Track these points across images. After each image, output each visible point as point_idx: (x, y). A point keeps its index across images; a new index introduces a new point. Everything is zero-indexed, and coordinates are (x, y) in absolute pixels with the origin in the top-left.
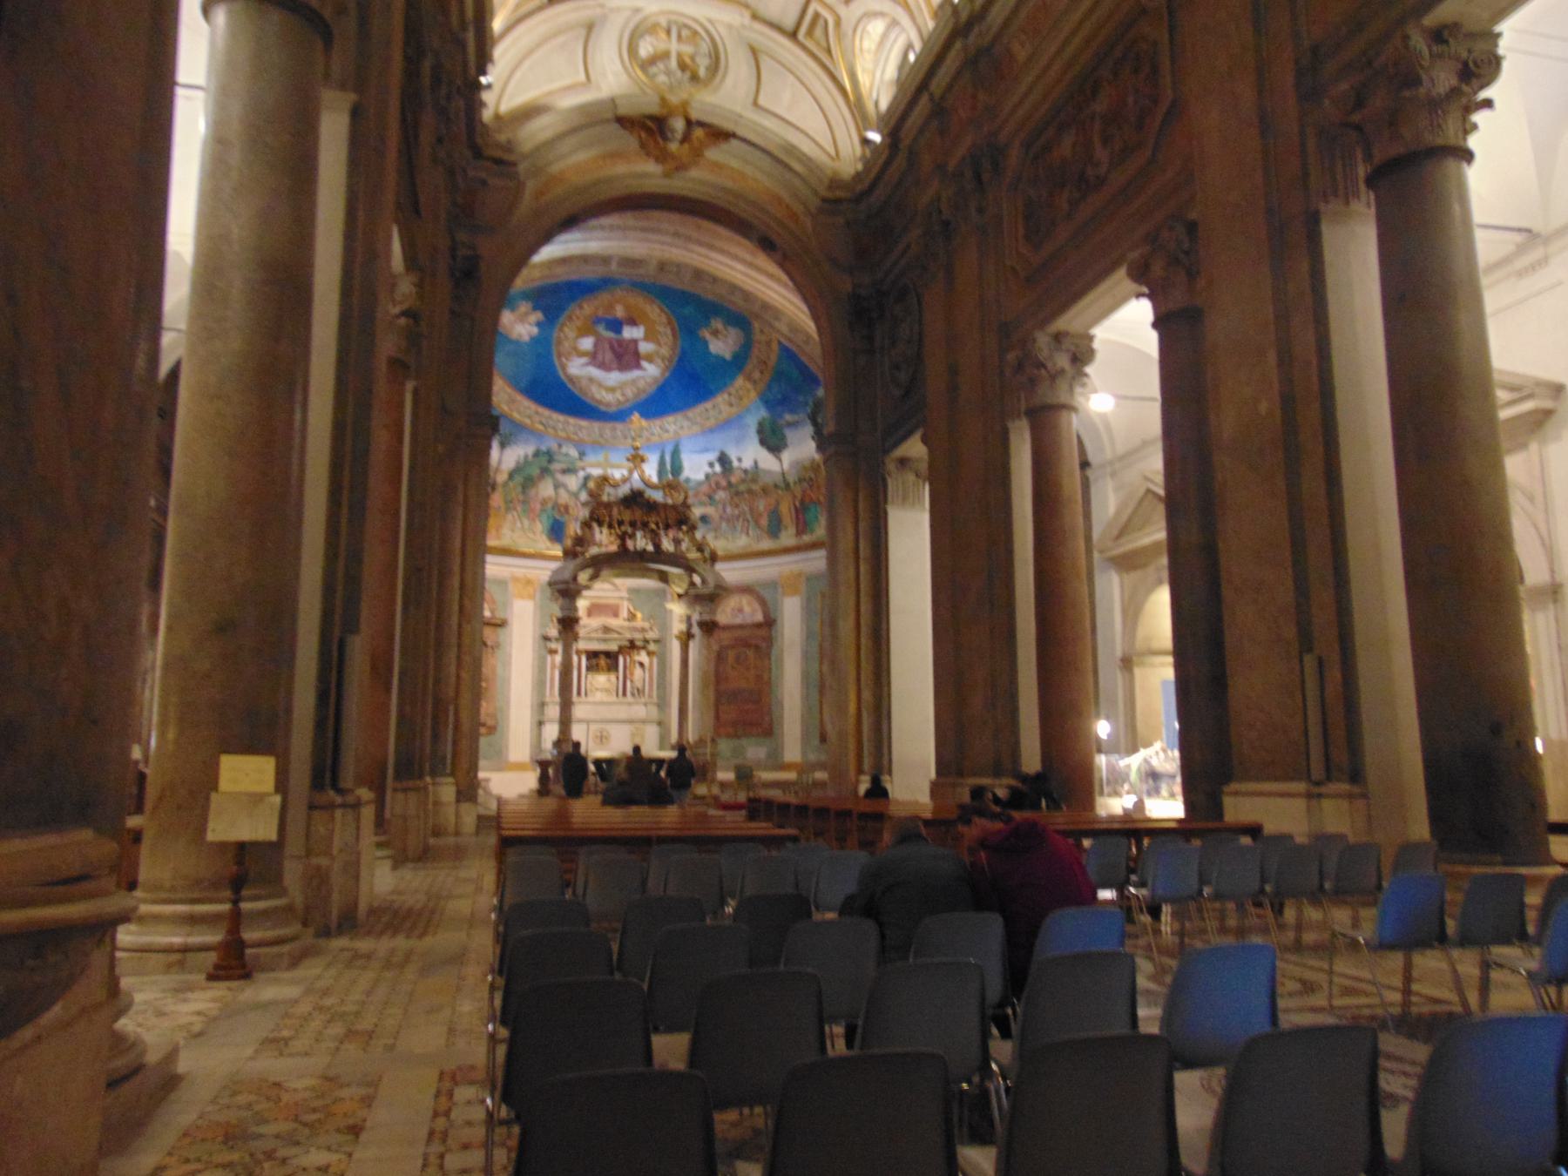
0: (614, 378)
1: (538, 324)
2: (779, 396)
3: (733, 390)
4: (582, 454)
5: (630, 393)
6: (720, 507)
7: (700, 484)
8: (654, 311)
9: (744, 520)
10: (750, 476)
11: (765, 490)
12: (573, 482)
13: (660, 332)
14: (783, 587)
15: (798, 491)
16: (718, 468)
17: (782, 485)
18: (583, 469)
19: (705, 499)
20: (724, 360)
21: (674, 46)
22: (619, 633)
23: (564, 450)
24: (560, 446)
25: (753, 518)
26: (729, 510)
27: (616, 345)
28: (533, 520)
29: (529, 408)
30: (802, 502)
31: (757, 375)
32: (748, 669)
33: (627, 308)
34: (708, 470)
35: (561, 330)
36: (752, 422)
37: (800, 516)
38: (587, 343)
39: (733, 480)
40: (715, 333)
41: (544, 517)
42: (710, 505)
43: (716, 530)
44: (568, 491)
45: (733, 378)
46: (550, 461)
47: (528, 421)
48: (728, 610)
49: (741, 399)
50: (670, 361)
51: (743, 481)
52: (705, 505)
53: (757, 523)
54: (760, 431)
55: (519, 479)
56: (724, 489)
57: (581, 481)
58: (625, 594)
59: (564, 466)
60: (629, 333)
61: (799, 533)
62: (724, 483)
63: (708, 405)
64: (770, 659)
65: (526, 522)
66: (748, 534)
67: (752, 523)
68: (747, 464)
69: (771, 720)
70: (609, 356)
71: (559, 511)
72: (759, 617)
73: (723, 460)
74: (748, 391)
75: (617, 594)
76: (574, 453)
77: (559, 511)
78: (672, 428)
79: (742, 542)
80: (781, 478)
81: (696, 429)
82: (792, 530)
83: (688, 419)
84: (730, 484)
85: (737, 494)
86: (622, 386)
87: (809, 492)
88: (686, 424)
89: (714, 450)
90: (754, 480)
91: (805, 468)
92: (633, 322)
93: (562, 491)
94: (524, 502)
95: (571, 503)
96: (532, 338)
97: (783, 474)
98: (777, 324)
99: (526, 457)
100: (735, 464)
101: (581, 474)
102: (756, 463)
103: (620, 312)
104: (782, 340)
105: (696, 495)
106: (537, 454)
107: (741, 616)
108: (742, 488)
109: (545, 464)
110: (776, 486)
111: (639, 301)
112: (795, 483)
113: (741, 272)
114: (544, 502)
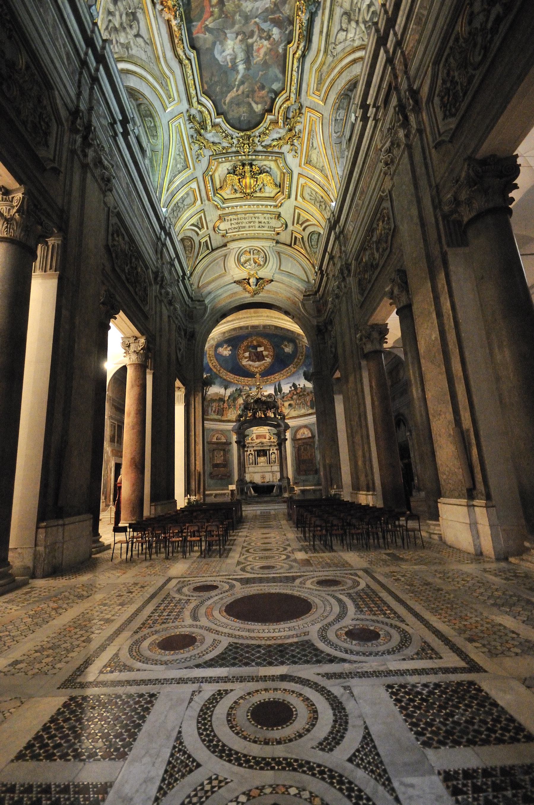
0: (257, 364)
1: (231, 350)
4: (250, 389)
5: (263, 368)
7: (288, 394)
8: (265, 342)
21: (252, 256)
31: (300, 357)
33: (257, 342)
36: (301, 372)
38: (247, 354)
40: (286, 346)
43: (294, 408)
45: (294, 359)
46: (241, 392)
55: (232, 398)
60: (259, 349)
68: (302, 386)
70: (254, 358)
72: (310, 435)
73: (294, 385)
76: (248, 389)
78: (277, 377)
79: (303, 411)
86: (260, 366)
90: (305, 391)
92: (260, 346)
94: (234, 405)
103: (255, 343)
106: (236, 390)
111: (261, 339)
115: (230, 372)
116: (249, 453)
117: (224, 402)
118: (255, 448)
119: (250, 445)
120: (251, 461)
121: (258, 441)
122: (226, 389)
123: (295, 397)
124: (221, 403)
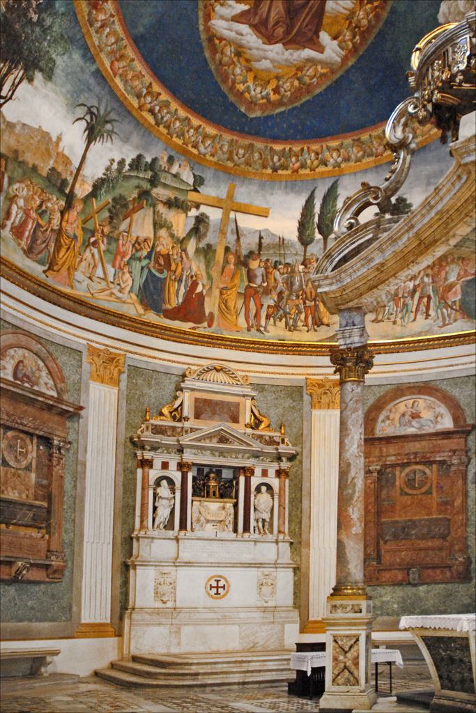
4: (199, 181)
9: (421, 298)
12: (181, 223)
18: (197, 207)
23: (175, 169)
24: (171, 160)
29: (139, 76)
44: (172, 236)
46: (154, 182)
47: (135, 103)
53: (443, 298)
55: (106, 198)
57: (191, 223)
66: (428, 316)
76: (188, 177)
77: (157, 261)
93: (163, 232)
94: (112, 239)
95: (175, 254)
99: (122, 163)
101: (193, 213)
106: (137, 163)
109: (146, 186)
114: (137, 244)
115: (137, 41)
117: (70, 199)
122: (92, 134)
124: (56, 203)
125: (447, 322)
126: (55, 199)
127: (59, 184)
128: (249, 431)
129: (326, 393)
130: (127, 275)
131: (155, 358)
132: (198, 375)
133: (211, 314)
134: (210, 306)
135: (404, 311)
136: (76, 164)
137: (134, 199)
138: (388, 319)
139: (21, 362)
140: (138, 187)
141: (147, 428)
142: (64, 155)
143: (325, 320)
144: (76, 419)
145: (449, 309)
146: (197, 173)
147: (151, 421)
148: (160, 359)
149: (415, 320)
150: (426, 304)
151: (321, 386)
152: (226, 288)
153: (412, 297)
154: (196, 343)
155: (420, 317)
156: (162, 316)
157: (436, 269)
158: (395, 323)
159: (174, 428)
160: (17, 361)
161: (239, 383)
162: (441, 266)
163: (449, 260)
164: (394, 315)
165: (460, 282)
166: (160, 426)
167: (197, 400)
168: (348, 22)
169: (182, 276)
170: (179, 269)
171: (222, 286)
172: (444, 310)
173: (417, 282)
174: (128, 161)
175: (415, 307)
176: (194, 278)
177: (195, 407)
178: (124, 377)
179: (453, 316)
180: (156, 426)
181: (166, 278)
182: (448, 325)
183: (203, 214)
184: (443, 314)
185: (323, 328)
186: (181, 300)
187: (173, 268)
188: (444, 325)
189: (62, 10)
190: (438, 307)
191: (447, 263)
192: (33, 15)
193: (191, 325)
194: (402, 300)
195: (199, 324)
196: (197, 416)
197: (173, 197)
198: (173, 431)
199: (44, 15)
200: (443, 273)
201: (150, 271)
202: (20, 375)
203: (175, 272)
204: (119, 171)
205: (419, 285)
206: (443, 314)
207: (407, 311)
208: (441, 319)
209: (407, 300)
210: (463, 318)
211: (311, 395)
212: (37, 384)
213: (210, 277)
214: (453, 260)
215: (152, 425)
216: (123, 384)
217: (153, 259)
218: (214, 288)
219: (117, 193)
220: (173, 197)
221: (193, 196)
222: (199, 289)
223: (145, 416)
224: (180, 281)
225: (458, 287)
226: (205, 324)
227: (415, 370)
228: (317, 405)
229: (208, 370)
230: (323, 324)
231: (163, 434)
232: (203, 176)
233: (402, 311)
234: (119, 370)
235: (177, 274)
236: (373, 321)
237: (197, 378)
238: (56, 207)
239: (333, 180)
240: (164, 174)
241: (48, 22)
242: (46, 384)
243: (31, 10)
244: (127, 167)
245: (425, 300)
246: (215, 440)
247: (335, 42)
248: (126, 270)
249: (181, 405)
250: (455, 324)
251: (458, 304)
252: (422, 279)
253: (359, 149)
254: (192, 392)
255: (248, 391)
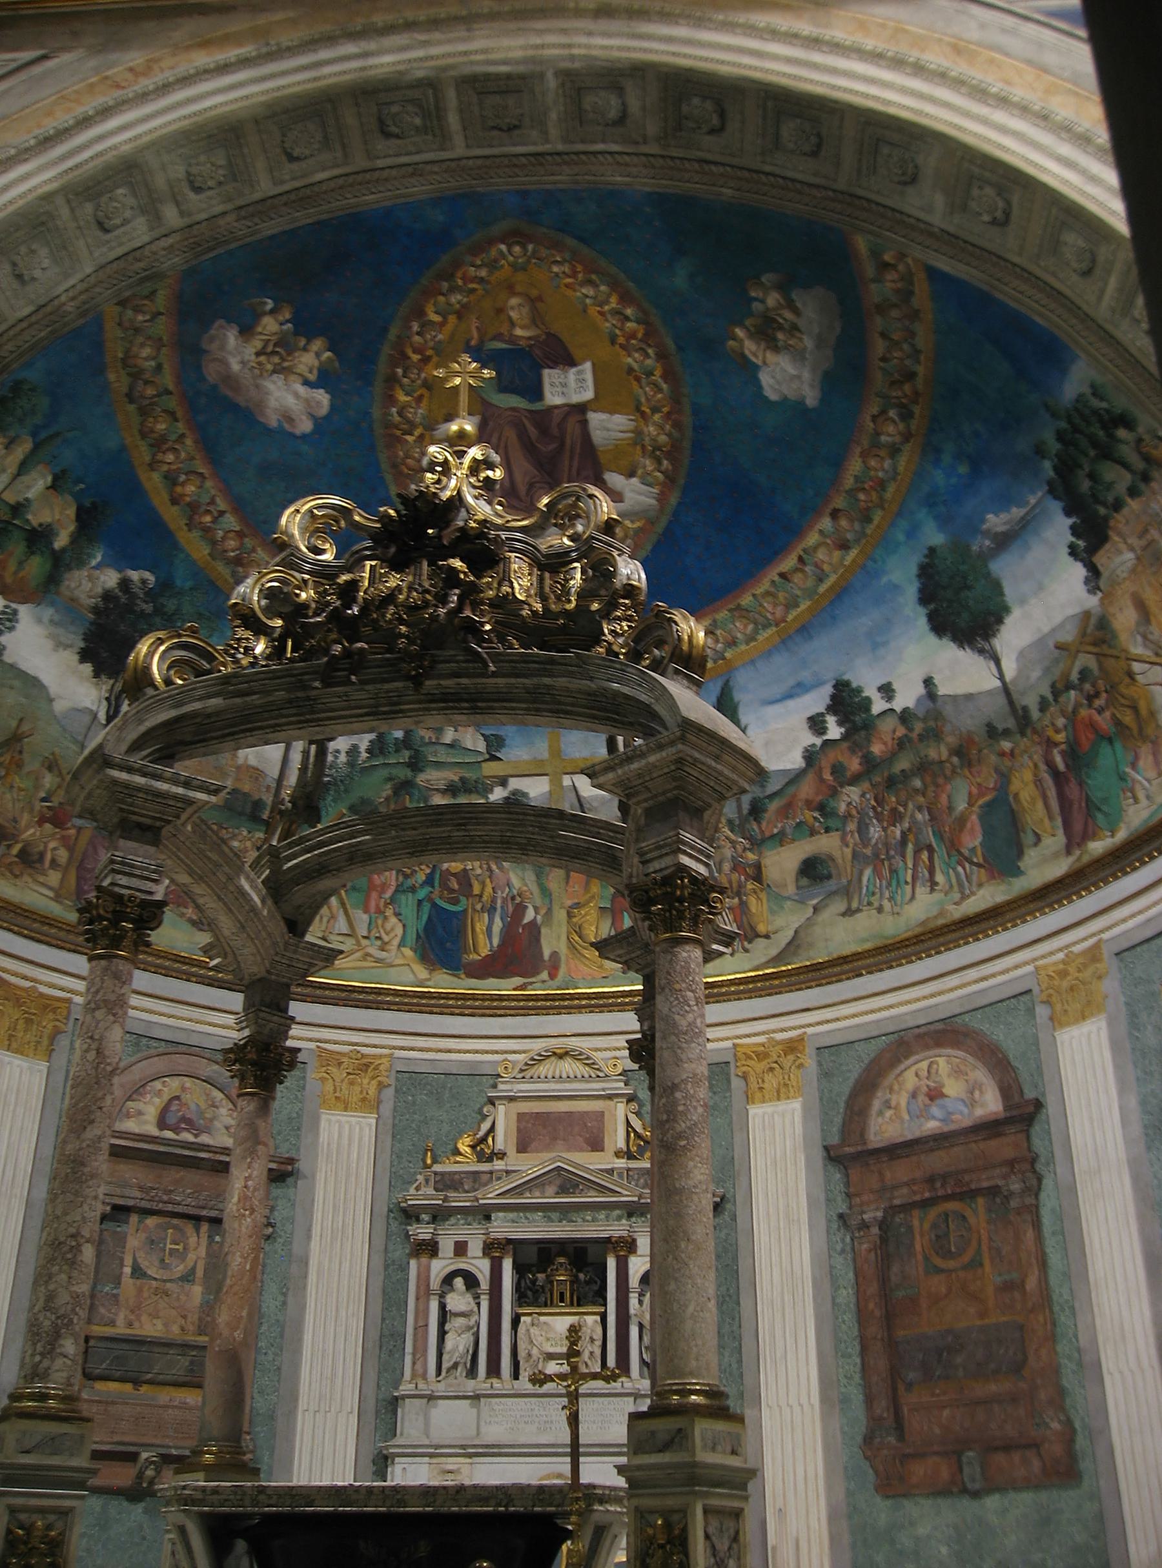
1: (324, 379)
2: (963, 469)
3: (839, 502)
4: (495, 744)
6: (852, 826)
7: (796, 778)
9: (917, 852)
10: (918, 727)
11: (964, 753)
13: (630, 370)
14: (1048, 1002)
15: (1058, 730)
16: (834, 731)
17: (1011, 723)
18: (503, 782)
19: (809, 815)
20: (800, 403)
22: (603, 1189)
25: (939, 835)
26: (875, 832)
27: (533, 431)
28: (379, 911)
30: (1073, 754)
32: (976, 1264)
34: (812, 740)
35: (391, 400)
37: (1073, 791)
39: (877, 749)
41: (408, 903)
42: (827, 830)
43: (846, 892)
45: (838, 463)
48: (903, 1100)
49: (867, 519)
50: (669, 455)
51: (902, 744)
52: (813, 833)
53: (953, 847)
54: (925, 598)
56: (854, 780)
58: (619, 1086)
59: (452, 776)
61: (1074, 841)
62: (854, 765)
63: (788, 563)
64: (1037, 1225)
65: (362, 919)
66: (933, 884)
67: (940, 852)
68: (907, 697)
69: (1069, 1423)
71: (444, 885)
72: (991, 1104)
74: (882, 485)
75: (596, 1087)
77: (444, 885)
80: (1002, 701)
81: (764, 635)
82: (1055, 841)
83: (741, 612)
84: (870, 765)
85: (891, 783)
87: (1084, 712)
88: (740, 628)
89: (819, 684)
90: (933, 734)
91: (1059, 647)
96: (319, 423)
97: (1006, 689)
98: (912, 202)
100: (879, 706)
102: (928, 682)
104: (943, 264)
105: (786, 811)
107: (935, 1111)
108: (903, 764)
109: (404, 773)
110: (992, 732)
112: (1043, 705)
113: (789, 61)
116: (439, 1267)
118: (502, 1227)
119: (459, 1200)
120: (458, 1343)
121: (531, 1165)
123: (852, 794)
125: (967, 892)
126: (245, 833)
127: (248, 810)
128: (621, 1163)
129: (771, 1069)
130: (393, 920)
131: (449, 1051)
132: (522, 1071)
133: (555, 955)
134: (553, 941)
135: (894, 883)
136: (275, 773)
137: (387, 799)
138: (869, 904)
139: (177, 1098)
140: (390, 779)
141: (427, 1181)
142: (249, 767)
143: (761, 928)
144: (290, 1180)
145: (967, 865)
146: (487, 733)
147: (437, 1168)
148: (459, 1051)
149: (913, 897)
150: (927, 862)
151: (761, 1056)
152: (578, 905)
153: (903, 856)
154: (524, 1011)
155: (922, 891)
156: (463, 976)
157: (931, 794)
158: (880, 910)
159: (476, 1173)
160: (166, 1097)
161: (601, 1074)
162: (937, 785)
163: (948, 773)
164: (878, 896)
165: (975, 809)
166: (450, 1173)
167: (521, 1116)
168: (638, 448)
169: (494, 900)
170: (489, 889)
171: (569, 903)
172: (960, 869)
173: (907, 825)
174: (364, 746)
175: (910, 872)
176: (518, 900)
177: (519, 1130)
178: (389, 1093)
179: (974, 878)
180: (443, 1174)
181: (465, 911)
182: (968, 897)
183: (515, 792)
184: (957, 875)
185: (760, 943)
186: (496, 942)
187: (476, 890)
188: (964, 897)
189: (189, 584)
190: (948, 865)
191: (946, 777)
192: (144, 606)
193: (518, 981)
194: (886, 863)
195: (533, 976)
196: (522, 1148)
197: (456, 779)
198: (474, 1182)
199: (163, 600)
200: (944, 799)
201: (434, 905)
202: (171, 1120)
203: (481, 896)
204: (351, 764)
205: (909, 829)
206: (957, 875)
207: (898, 882)
208: (956, 888)
209: (893, 861)
210: (994, 878)
211: (745, 1077)
212: (207, 1130)
213: (545, 892)
214: (954, 772)
215: (436, 1173)
216: (387, 1108)
217: (437, 884)
218: (555, 907)
219: (353, 797)
220: (456, 779)
221: (490, 769)
222: (530, 915)
223: (424, 1161)
224: (491, 910)
225: (974, 817)
226: (545, 975)
227: (925, 998)
228: (758, 1095)
229: (541, 1059)
230: (758, 936)
231: (456, 1190)
232: (501, 732)
233: (889, 885)
234: (380, 1083)
235: (485, 898)
236: (844, 914)
237: (520, 1076)
238: (248, 844)
239: (719, 684)
240: (431, 749)
241: (171, 605)
242: (227, 1128)
243: (138, 602)
244: (364, 755)
245: (925, 856)
246: (551, 1190)
247: (634, 480)
248: (389, 912)
249: (492, 1129)
250: (981, 892)
251: (979, 853)
252: (912, 816)
253: (745, 621)
254: (512, 1105)
255: (619, 1086)
